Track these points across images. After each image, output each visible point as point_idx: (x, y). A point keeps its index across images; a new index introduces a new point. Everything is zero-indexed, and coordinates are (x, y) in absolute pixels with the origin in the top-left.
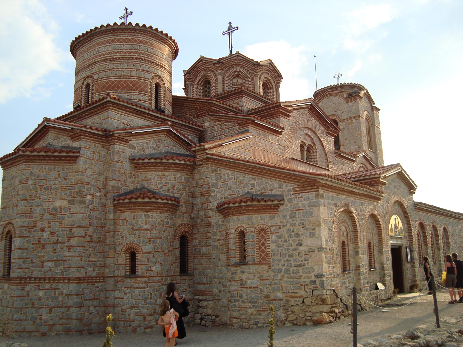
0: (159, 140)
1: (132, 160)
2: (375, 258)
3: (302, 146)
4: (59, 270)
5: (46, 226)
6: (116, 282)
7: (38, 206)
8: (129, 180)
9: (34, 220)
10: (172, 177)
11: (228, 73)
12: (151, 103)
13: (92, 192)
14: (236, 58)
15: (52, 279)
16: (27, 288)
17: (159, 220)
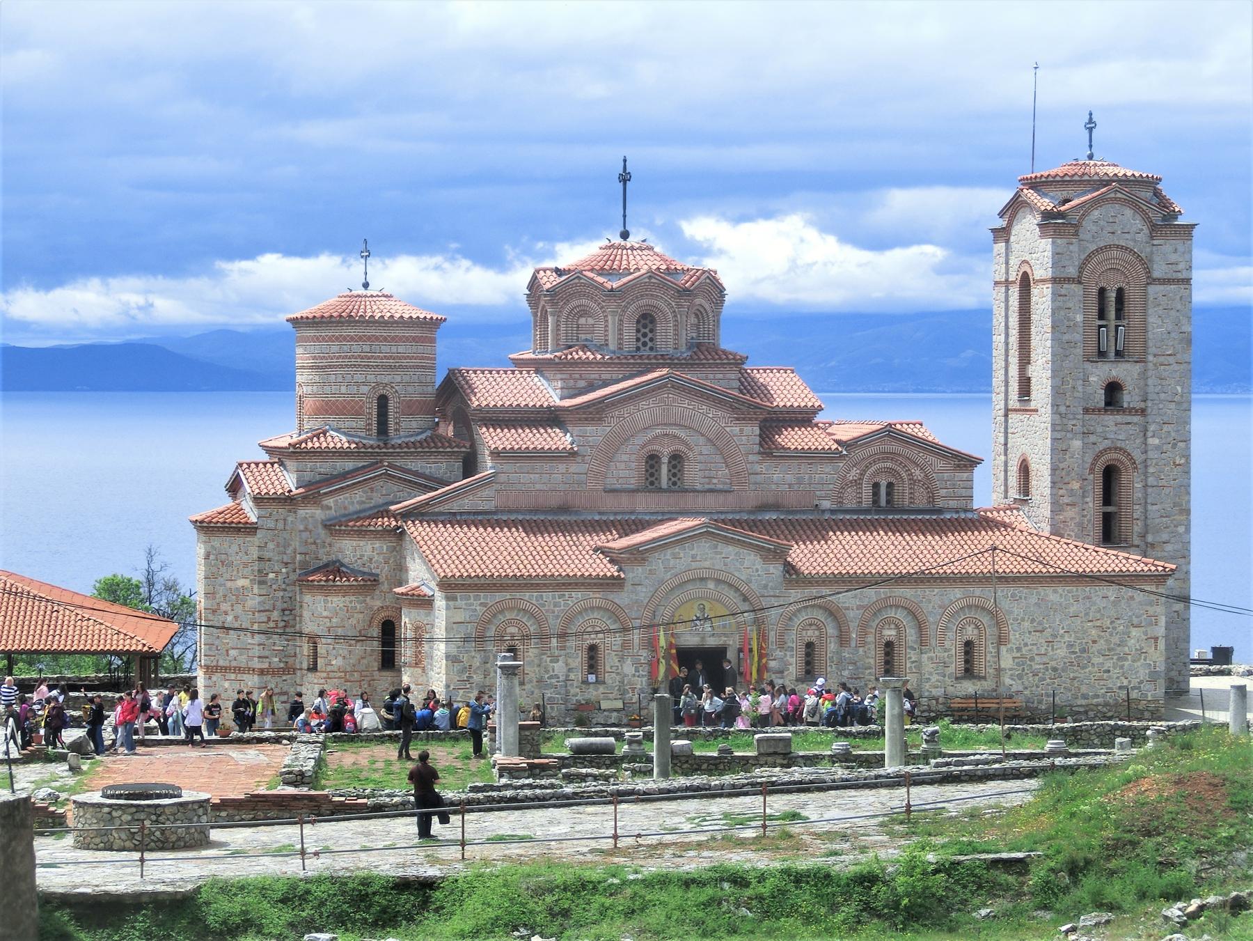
0: (372, 492)
1: (325, 526)
2: (608, 669)
3: (653, 460)
4: (242, 661)
5: (230, 608)
6: (303, 676)
7: (221, 585)
8: (321, 551)
9: (217, 601)
10: (369, 547)
11: (567, 309)
12: (371, 430)
13: (276, 568)
14: (576, 281)
15: (238, 670)
16: (214, 678)
17: (341, 605)
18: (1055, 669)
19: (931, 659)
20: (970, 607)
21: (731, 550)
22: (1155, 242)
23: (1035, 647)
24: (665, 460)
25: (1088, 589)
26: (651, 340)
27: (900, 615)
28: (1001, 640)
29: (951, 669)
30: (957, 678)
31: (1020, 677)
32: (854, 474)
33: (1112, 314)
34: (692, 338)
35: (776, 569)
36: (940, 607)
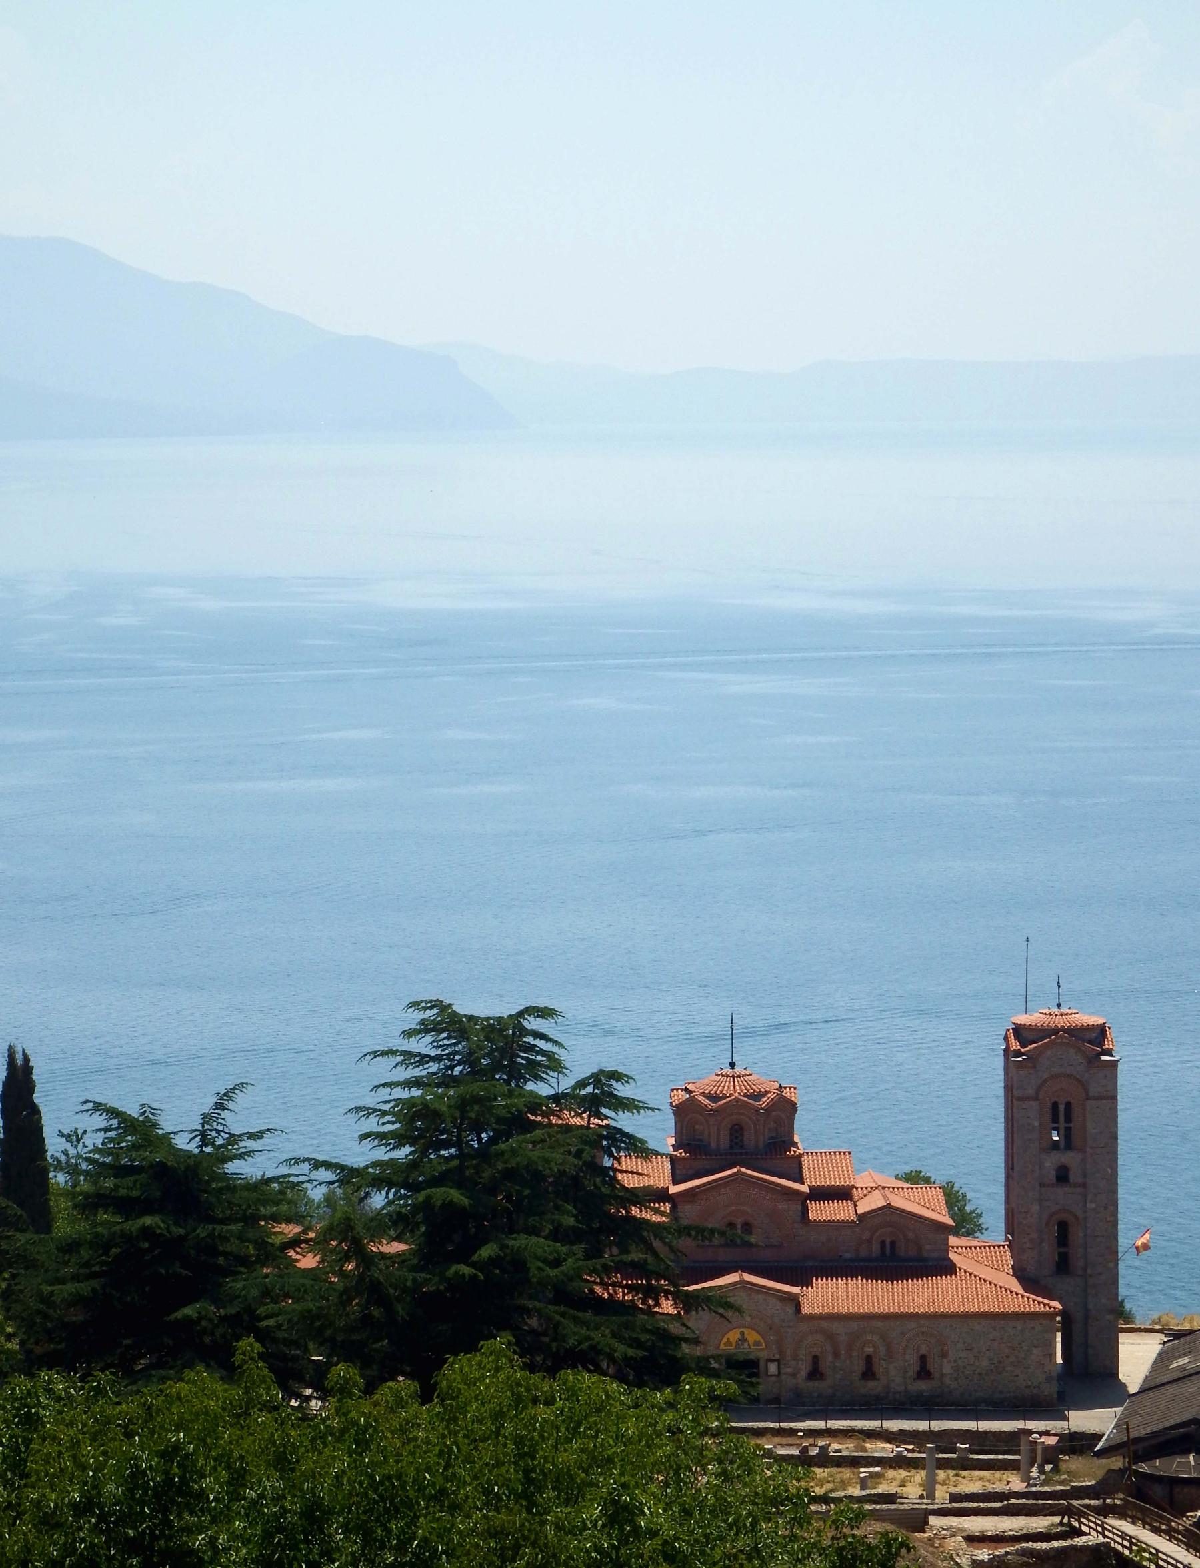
18: (980, 1374)
19: (896, 1367)
20: (923, 1333)
21: (760, 1297)
22: (1091, 1072)
23: (966, 1360)
24: (739, 1226)
25: (1002, 1322)
26: (742, 1140)
27: (875, 1338)
28: (944, 1355)
29: (910, 1374)
30: (914, 1379)
31: (956, 1379)
32: (866, 1235)
33: (1062, 1119)
34: (772, 1138)
35: (790, 1310)
36: (902, 1333)
